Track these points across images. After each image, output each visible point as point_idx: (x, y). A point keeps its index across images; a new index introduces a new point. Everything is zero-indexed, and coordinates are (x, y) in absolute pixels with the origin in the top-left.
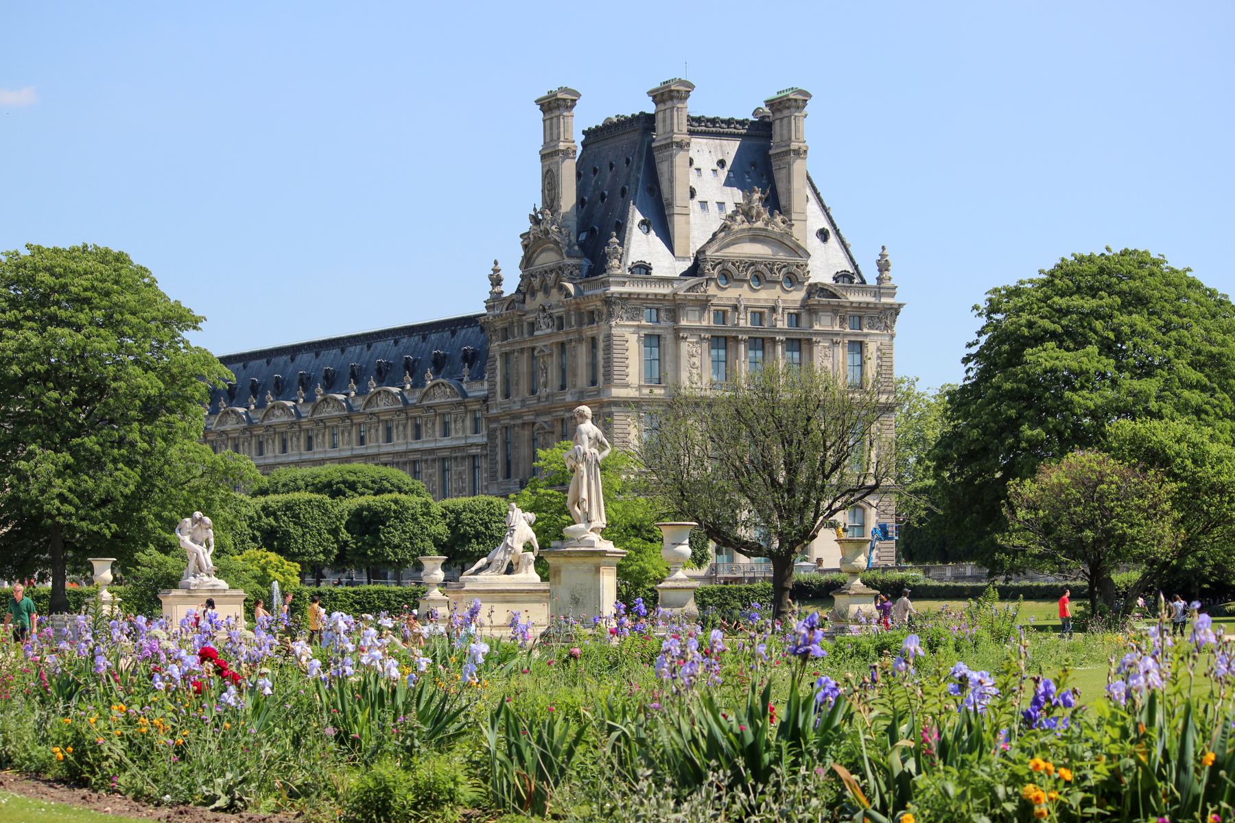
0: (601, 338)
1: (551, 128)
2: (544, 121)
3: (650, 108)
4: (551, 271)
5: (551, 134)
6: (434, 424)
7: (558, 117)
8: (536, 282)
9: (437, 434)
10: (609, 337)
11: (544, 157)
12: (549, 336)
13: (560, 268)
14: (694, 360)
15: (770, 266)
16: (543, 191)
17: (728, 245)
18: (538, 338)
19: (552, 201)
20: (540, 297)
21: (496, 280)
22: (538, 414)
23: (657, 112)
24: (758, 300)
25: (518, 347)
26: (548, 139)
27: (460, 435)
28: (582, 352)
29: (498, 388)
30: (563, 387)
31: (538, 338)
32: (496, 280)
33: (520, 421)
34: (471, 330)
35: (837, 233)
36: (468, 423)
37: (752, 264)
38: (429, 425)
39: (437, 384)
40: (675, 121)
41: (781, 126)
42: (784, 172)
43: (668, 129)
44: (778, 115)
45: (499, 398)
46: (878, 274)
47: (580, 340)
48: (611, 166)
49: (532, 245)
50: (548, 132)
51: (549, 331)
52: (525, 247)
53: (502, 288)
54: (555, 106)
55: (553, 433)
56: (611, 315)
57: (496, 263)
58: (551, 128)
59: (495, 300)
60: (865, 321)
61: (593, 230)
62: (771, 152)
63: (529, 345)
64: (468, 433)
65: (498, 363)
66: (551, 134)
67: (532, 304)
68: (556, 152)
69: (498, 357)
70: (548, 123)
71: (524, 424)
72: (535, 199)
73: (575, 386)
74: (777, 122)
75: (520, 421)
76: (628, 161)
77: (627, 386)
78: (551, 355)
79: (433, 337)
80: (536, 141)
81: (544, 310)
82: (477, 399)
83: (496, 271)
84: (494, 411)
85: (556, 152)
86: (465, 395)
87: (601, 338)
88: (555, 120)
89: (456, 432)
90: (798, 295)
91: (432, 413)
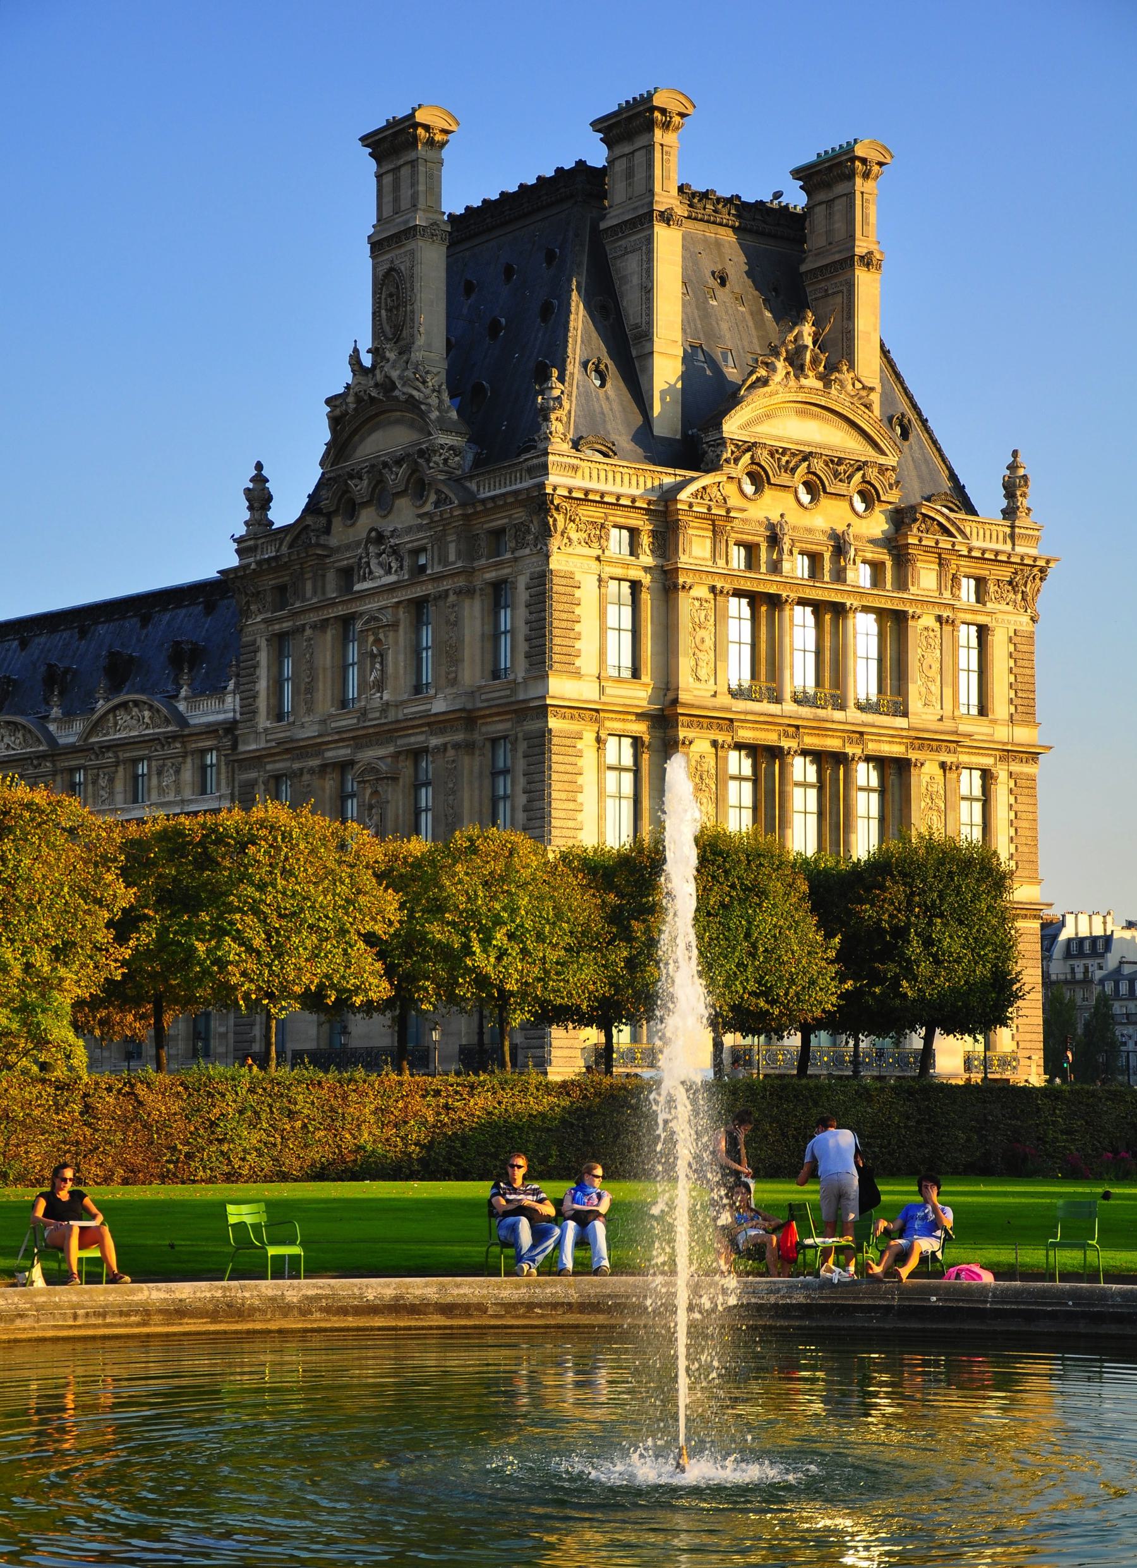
0: (522, 581)
1: (396, 187)
2: (379, 177)
3: (597, 155)
4: (399, 462)
5: (396, 200)
6: (111, 780)
7: (413, 163)
8: (361, 488)
9: (119, 798)
10: (541, 580)
11: (377, 246)
12: (391, 588)
13: (421, 453)
14: (702, 633)
15: (834, 462)
16: (376, 314)
17: (758, 420)
18: (364, 595)
19: (398, 329)
20: (367, 518)
21: (259, 497)
22: (360, 741)
23: (611, 161)
24: (810, 530)
25: (314, 618)
26: (387, 211)
27: (171, 798)
28: (473, 616)
29: (262, 704)
30: (418, 689)
31: (364, 595)
32: (259, 497)
33: (315, 762)
34: (182, 612)
35: (924, 422)
36: (187, 775)
37: (806, 457)
38: (103, 782)
39: (124, 705)
40: (658, 172)
41: (830, 216)
42: (839, 299)
43: (640, 188)
44: (822, 196)
45: (263, 721)
46: (1004, 503)
47: (470, 592)
48: (509, 271)
49: (350, 417)
50: (388, 198)
51: (392, 578)
52: (336, 422)
53: (271, 515)
54: (397, 146)
55: (395, 779)
56: (546, 532)
57: (259, 466)
58: (396, 187)
59: (258, 534)
60: (992, 588)
61: (478, 389)
62: (803, 268)
63: (341, 611)
64: (188, 794)
65: (263, 657)
66: (396, 200)
67: (341, 534)
68: (411, 232)
69: (263, 643)
70: (388, 179)
71: (324, 768)
72: (358, 329)
73: (454, 682)
74: (820, 211)
75: (315, 762)
76: (550, 257)
77: (577, 674)
78: (394, 626)
79: (102, 629)
80: (363, 216)
81: (380, 538)
82: (211, 730)
83: (260, 479)
84: (251, 746)
85: (411, 232)
86: (182, 721)
87: (522, 581)
88: (405, 172)
89: (162, 791)
90: (877, 525)
91: (110, 758)
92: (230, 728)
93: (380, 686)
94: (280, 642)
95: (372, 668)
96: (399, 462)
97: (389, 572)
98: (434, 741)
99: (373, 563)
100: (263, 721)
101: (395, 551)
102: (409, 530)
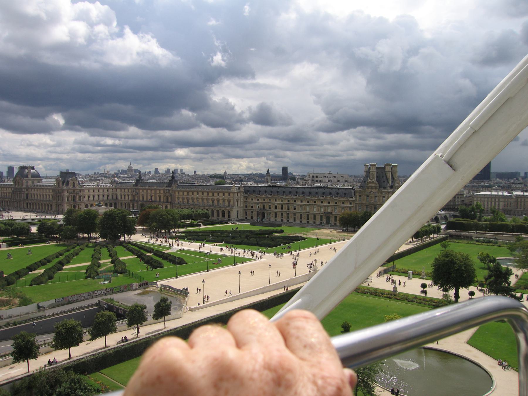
20: (370, 190)
92: (354, 201)
94: (360, 196)
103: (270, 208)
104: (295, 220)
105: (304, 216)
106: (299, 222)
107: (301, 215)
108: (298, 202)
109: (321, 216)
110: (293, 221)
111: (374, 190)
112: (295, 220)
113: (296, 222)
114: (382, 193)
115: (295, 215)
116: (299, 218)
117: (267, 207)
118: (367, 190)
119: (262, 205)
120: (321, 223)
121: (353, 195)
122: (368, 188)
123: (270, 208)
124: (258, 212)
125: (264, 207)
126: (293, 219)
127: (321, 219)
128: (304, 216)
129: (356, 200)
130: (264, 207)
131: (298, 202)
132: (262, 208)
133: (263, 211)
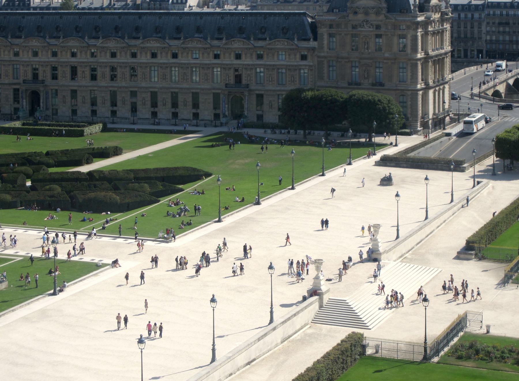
12: (372, 31)
13: (380, 8)
20: (361, 17)
28: (395, 39)
33: (347, 60)
45: (326, 49)
65: (326, 37)
81: (367, 21)
92: (313, 49)
93: (368, 49)
94: (331, 35)
95: (365, 45)
96: (373, 8)
97: (370, 27)
98: (385, 61)
99: (365, 26)
100: (326, 49)
101: (371, 25)
102: (375, 21)
103: (55, 77)
104: (134, 109)
105: (165, 98)
106: (148, 115)
107: (154, 95)
108: (144, 58)
109: (216, 97)
110: (128, 114)
111: (372, 17)
112: (134, 109)
113: (139, 114)
114: (395, 27)
115: (134, 94)
116: (149, 103)
117: (45, 74)
118: (351, 17)
119: (29, 69)
120: (217, 116)
121: (310, 35)
122: (356, 13)
123: (55, 77)
124: (16, 91)
125: (35, 76)
126: (129, 107)
127: (216, 106)
128: (165, 98)
129: (321, 47)
130: (35, 76)
131: (144, 58)
132: (30, 76)
133: (34, 87)
